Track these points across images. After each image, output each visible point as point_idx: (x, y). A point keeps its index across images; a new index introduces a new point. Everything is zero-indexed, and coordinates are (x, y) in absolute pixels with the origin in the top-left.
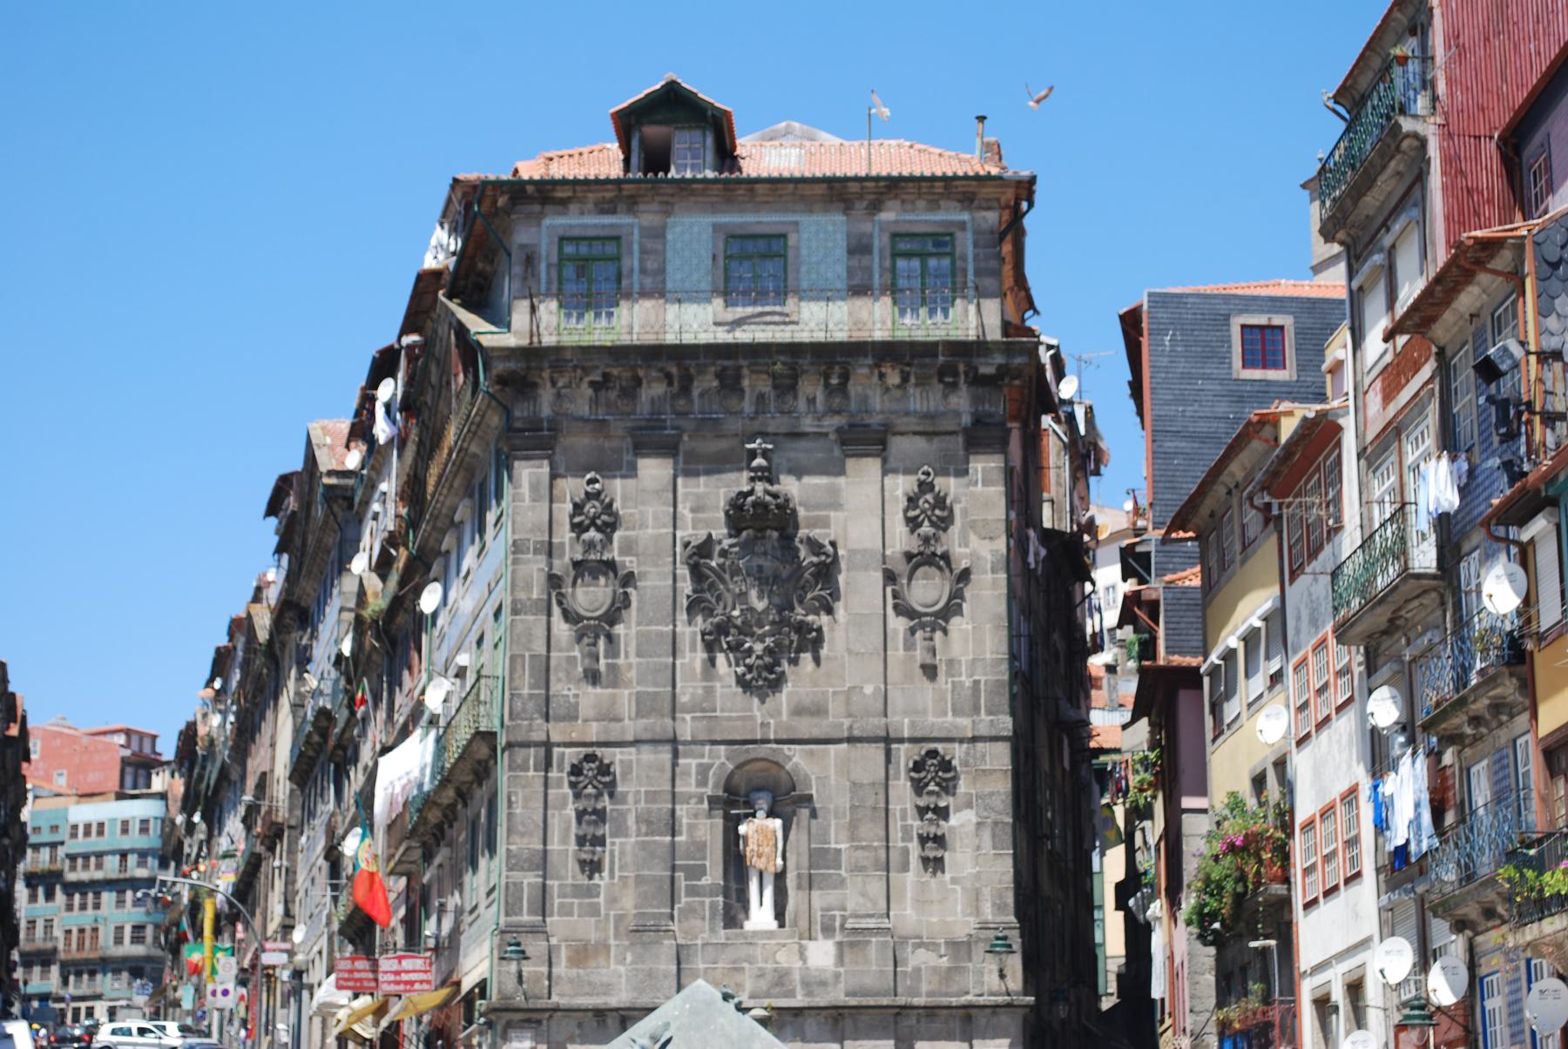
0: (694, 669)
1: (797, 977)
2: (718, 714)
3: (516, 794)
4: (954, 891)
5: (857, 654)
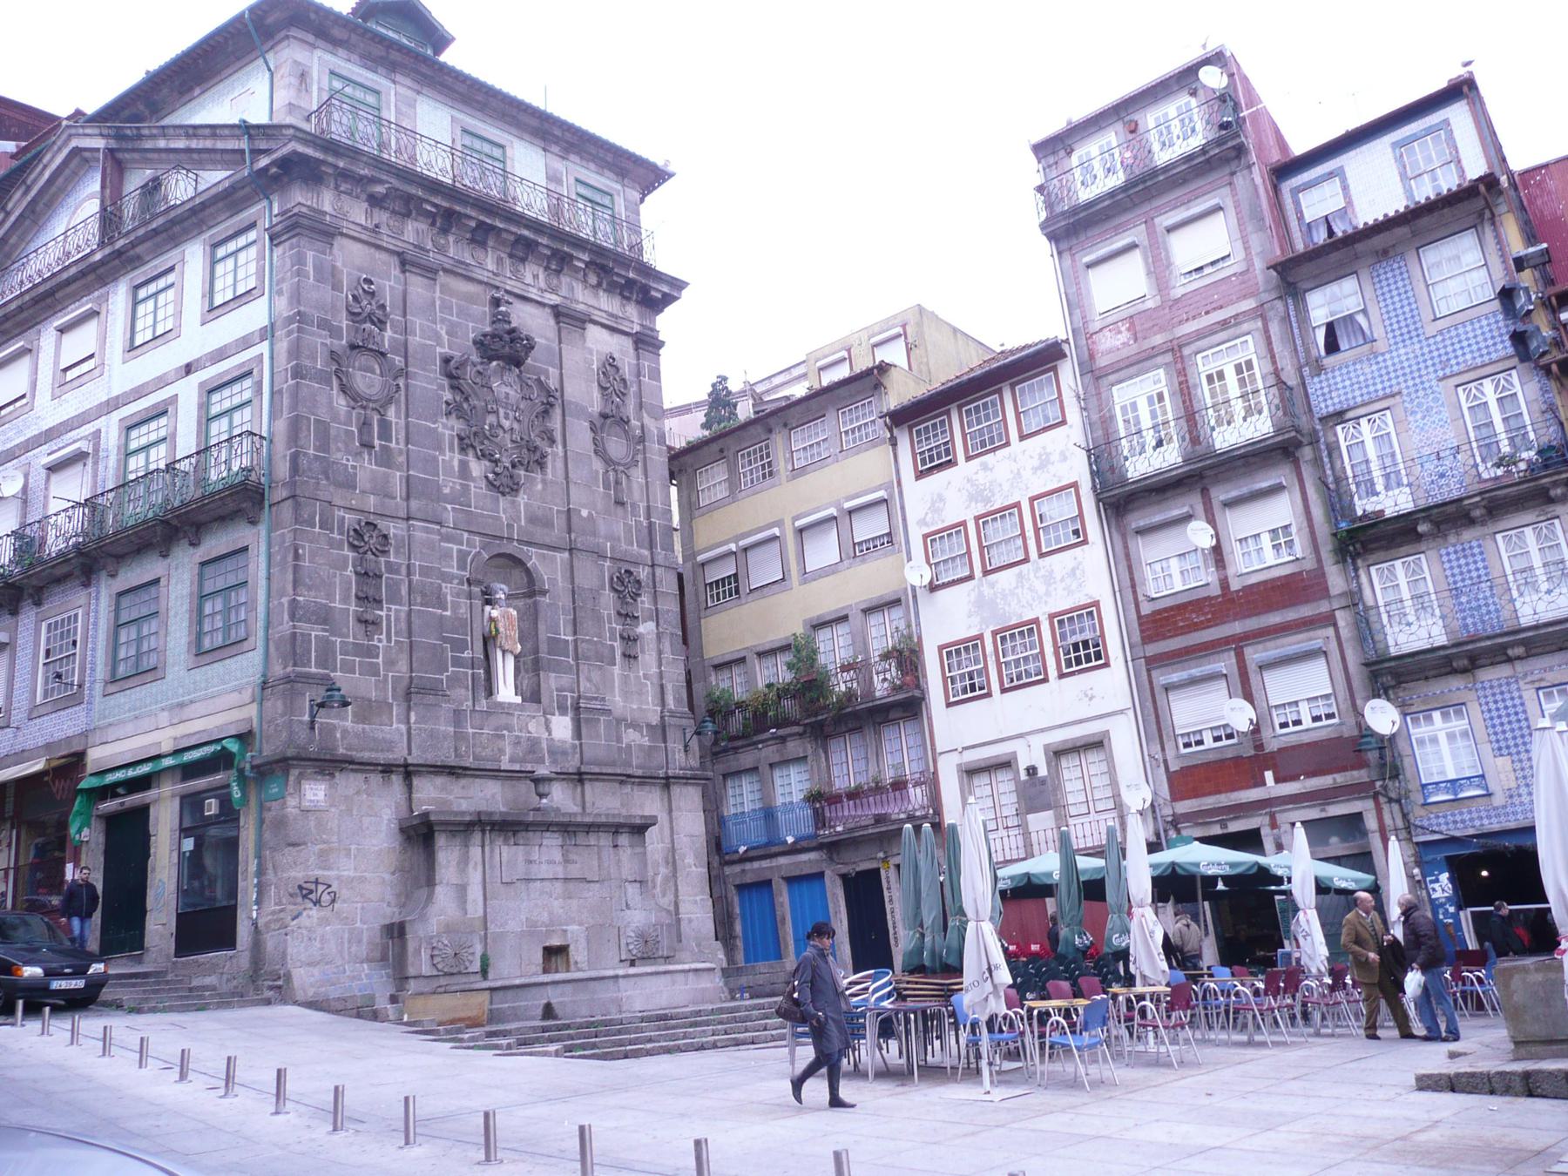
1: (544, 745)
3: (303, 547)
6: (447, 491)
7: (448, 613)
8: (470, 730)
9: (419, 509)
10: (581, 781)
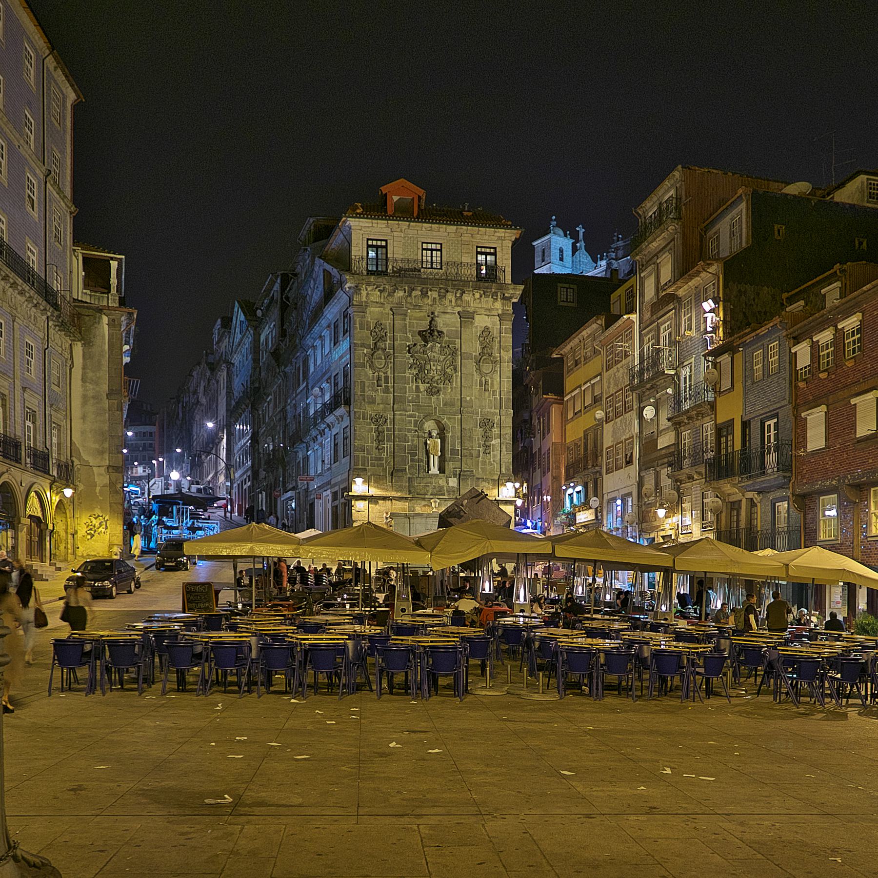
1: (445, 488)
6: (410, 398)
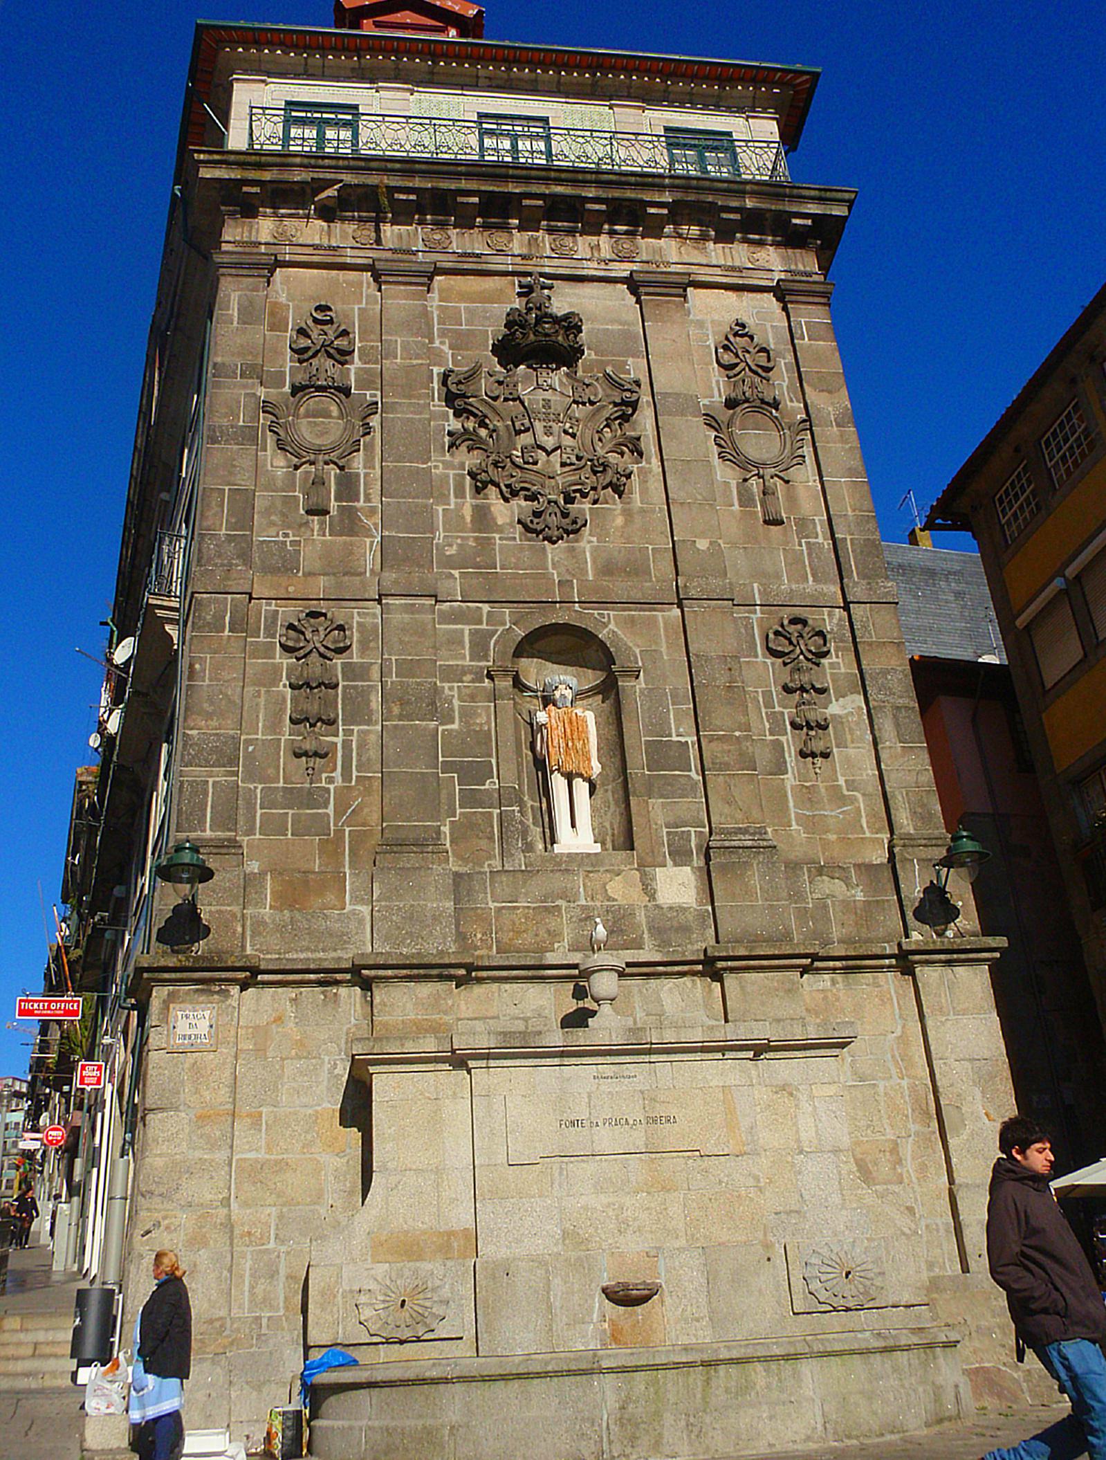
0: (463, 517)
1: (641, 918)
2: (498, 570)
3: (202, 661)
4: (856, 799)
5: (681, 504)
7: (455, 726)
8: (492, 905)
9: (396, 582)
10: (717, 976)
